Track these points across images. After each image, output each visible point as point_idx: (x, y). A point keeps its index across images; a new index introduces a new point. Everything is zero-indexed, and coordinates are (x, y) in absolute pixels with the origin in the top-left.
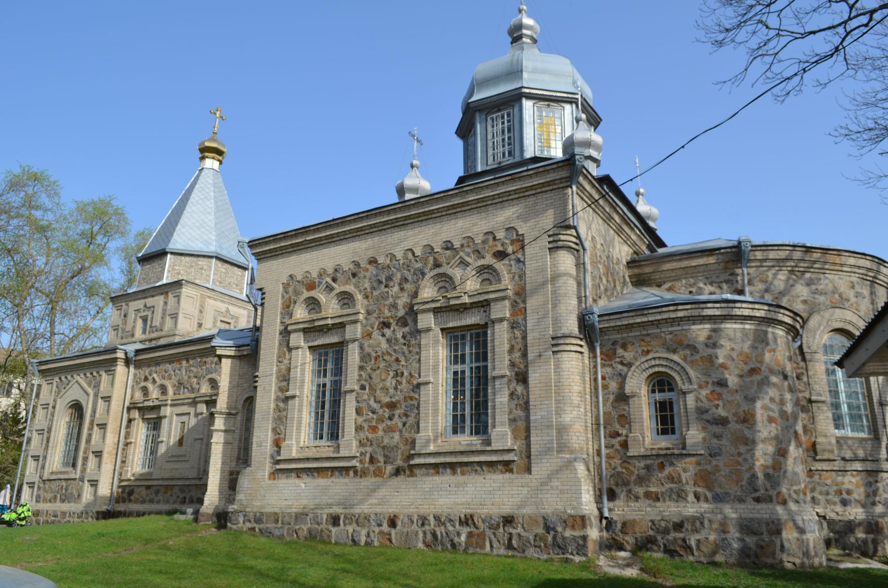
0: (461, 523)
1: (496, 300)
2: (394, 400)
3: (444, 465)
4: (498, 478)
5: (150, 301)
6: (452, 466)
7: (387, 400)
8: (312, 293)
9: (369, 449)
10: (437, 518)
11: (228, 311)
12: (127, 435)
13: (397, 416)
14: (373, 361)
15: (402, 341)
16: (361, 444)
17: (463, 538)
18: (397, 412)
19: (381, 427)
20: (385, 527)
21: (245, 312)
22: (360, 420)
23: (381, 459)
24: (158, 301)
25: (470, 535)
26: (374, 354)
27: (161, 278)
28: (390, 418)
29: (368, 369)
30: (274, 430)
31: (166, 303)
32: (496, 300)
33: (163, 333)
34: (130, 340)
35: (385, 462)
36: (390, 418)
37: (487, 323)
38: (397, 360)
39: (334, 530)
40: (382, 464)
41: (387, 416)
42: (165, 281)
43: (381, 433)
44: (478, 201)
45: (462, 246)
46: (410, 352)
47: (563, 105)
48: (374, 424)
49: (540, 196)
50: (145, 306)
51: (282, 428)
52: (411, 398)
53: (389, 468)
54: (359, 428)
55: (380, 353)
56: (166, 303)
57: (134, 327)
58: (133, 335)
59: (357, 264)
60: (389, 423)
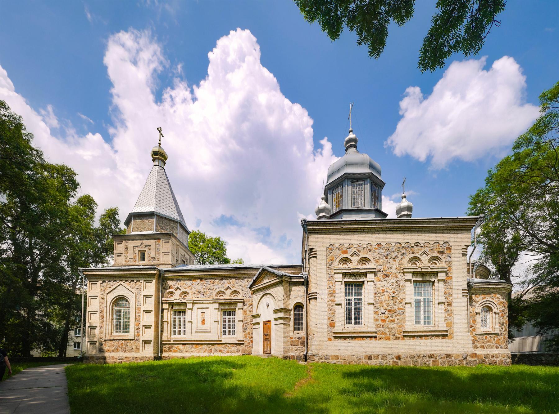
0: (429, 357)
3: (417, 336)
4: (440, 340)
6: (421, 336)
7: (389, 308)
10: (419, 356)
15: (396, 284)
17: (431, 362)
20: (395, 360)
22: (377, 317)
25: (433, 361)
26: (381, 288)
36: (391, 317)
39: (370, 362)
43: (387, 322)
52: (401, 309)
60: (391, 318)
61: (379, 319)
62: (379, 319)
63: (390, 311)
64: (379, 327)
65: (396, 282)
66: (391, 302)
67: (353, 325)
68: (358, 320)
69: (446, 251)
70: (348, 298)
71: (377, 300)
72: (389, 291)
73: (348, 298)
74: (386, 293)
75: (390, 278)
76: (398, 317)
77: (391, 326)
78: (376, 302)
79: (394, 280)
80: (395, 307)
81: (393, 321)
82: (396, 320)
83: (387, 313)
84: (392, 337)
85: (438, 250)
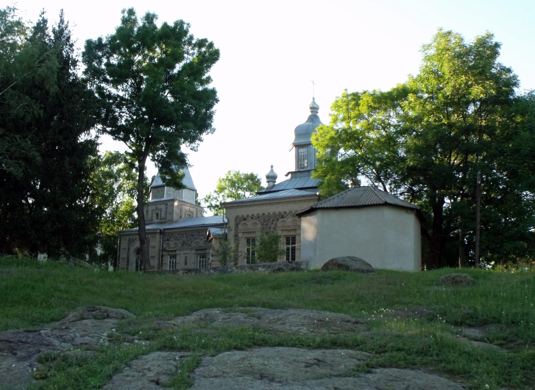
5: (159, 207)
8: (245, 222)
11: (189, 210)
12: (162, 261)
21: (195, 210)
24: (163, 207)
27: (163, 197)
31: (167, 208)
33: (167, 220)
34: (151, 222)
42: (165, 198)
50: (157, 208)
56: (167, 208)
57: (152, 217)
58: (152, 220)
59: (259, 214)
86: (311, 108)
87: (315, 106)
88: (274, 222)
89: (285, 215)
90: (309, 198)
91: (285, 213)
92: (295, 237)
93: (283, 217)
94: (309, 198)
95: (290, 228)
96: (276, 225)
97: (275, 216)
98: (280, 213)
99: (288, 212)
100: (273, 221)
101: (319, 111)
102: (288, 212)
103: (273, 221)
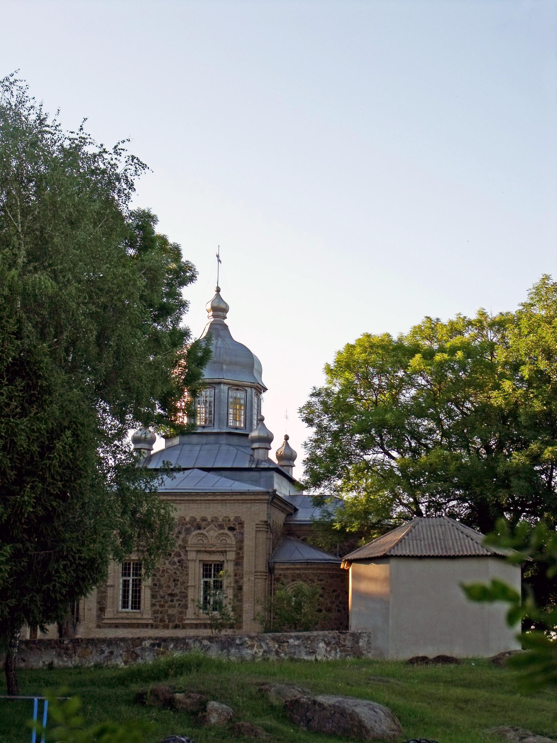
1: (230, 551)
2: (173, 592)
7: (170, 592)
9: (160, 616)
13: (175, 600)
14: (161, 572)
15: (178, 564)
16: (155, 612)
18: (175, 599)
19: (166, 605)
22: (154, 601)
23: (167, 621)
26: (161, 569)
28: (172, 601)
29: (158, 576)
30: (99, 603)
32: (230, 551)
35: (169, 622)
36: (172, 601)
37: (223, 561)
38: (175, 573)
40: (167, 622)
41: (170, 600)
43: (166, 608)
44: (222, 500)
45: (212, 521)
46: (183, 570)
47: (247, 389)
48: (162, 603)
49: (253, 504)
51: (104, 602)
52: (183, 592)
53: (171, 625)
54: (153, 605)
55: (165, 568)
60: (171, 603)
61: (158, 604)
62: (158, 604)
63: (171, 595)
64: (157, 613)
65: (179, 562)
66: (172, 584)
67: (129, 610)
68: (137, 605)
69: (237, 527)
70: (125, 578)
71: (156, 582)
72: (170, 571)
73: (125, 578)
74: (166, 574)
75: (172, 556)
76: (179, 602)
77: (170, 612)
78: (155, 585)
79: (176, 559)
80: (177, 591)
81: (174, 607)
82: (177, 605)
83: (166, 596)
84: (171, 625)
85: (229, 526)
86: (214, 309)
87: (223, 306)
88: (182, 536)
89: (203, 524)
90: (252, 497)
91: (204, 519)
92: (222, 565)
93: (199, 528)
94: (252, 497)
95: (214, 549)
96: (185, 541)
97: (183, 524)
98: (193, 519)
99: (209, 520)
100: (180, 533)
101: (228, 315)
102: (209, 520)
103: (180, 533)
